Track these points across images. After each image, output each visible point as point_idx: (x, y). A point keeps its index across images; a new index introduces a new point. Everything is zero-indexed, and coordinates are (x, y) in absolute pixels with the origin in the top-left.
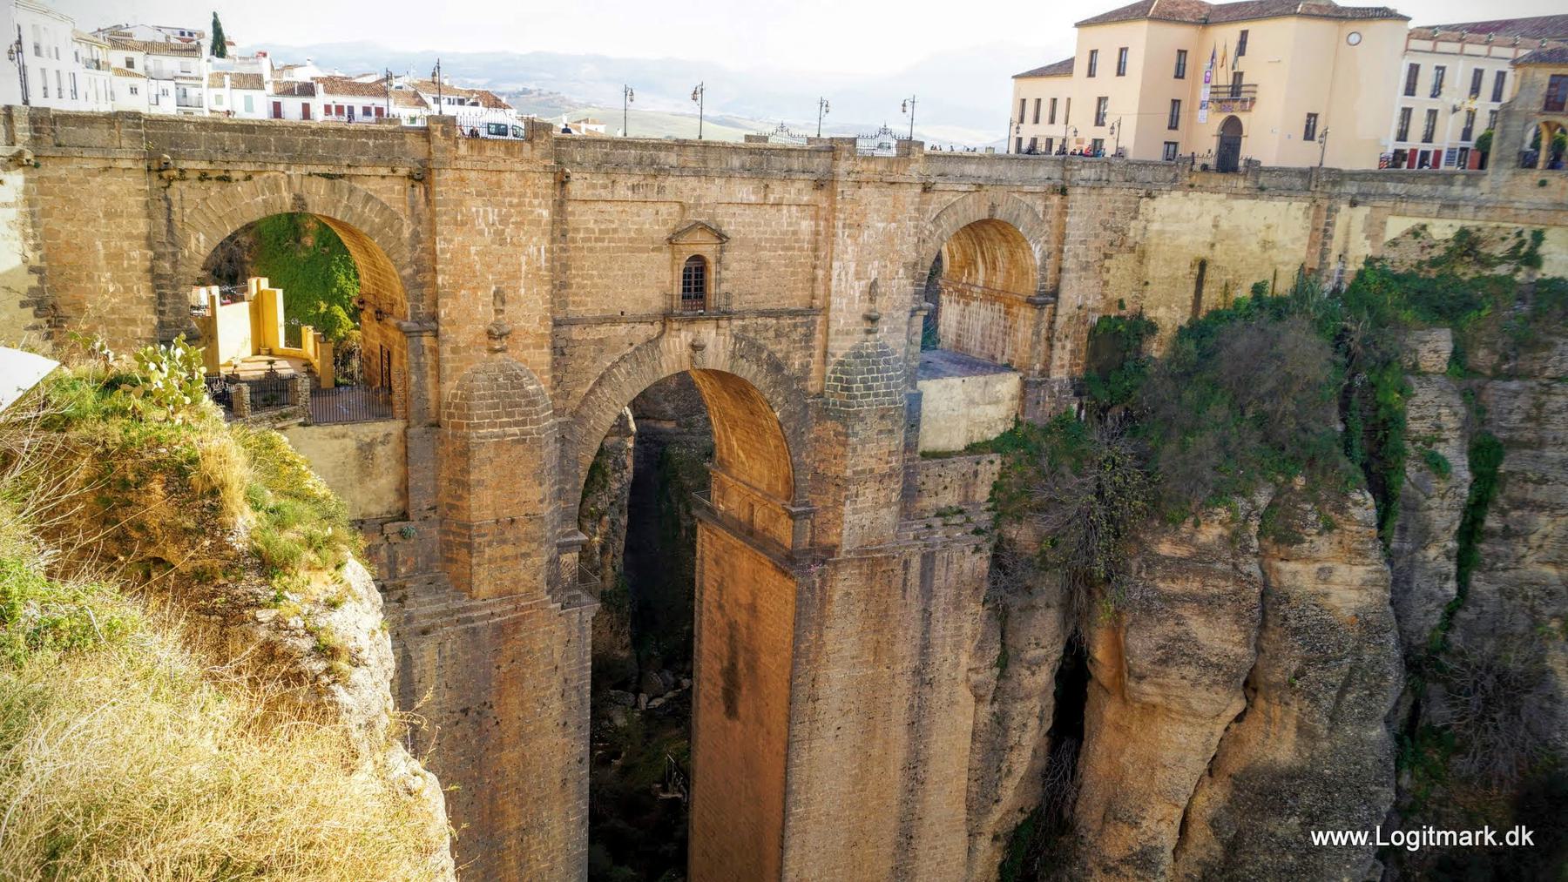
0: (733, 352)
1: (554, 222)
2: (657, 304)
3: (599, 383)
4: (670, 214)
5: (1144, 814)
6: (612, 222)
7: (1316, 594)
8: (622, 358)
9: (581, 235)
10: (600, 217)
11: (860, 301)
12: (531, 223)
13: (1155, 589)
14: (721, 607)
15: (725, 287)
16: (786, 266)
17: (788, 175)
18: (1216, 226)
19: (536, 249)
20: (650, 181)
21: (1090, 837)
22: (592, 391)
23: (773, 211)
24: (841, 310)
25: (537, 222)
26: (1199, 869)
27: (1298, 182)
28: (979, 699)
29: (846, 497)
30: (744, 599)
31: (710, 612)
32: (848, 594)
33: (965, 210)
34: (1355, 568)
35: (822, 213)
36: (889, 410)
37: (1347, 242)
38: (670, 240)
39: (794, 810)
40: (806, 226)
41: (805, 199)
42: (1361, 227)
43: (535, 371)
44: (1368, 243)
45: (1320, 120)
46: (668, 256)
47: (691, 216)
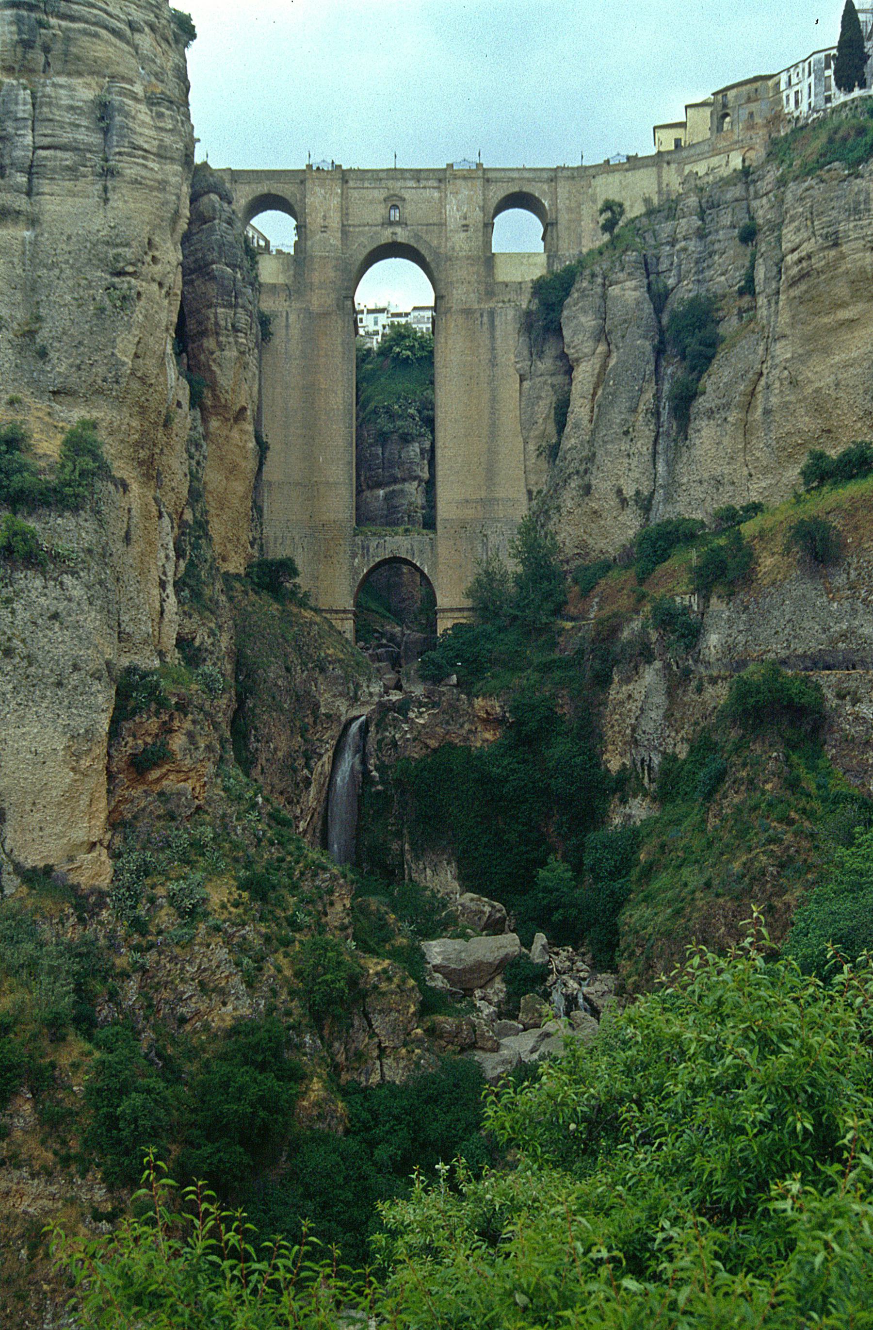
2: (380, 221)
19: (335, 202)
40: (436, 195)
41: (435, 185)
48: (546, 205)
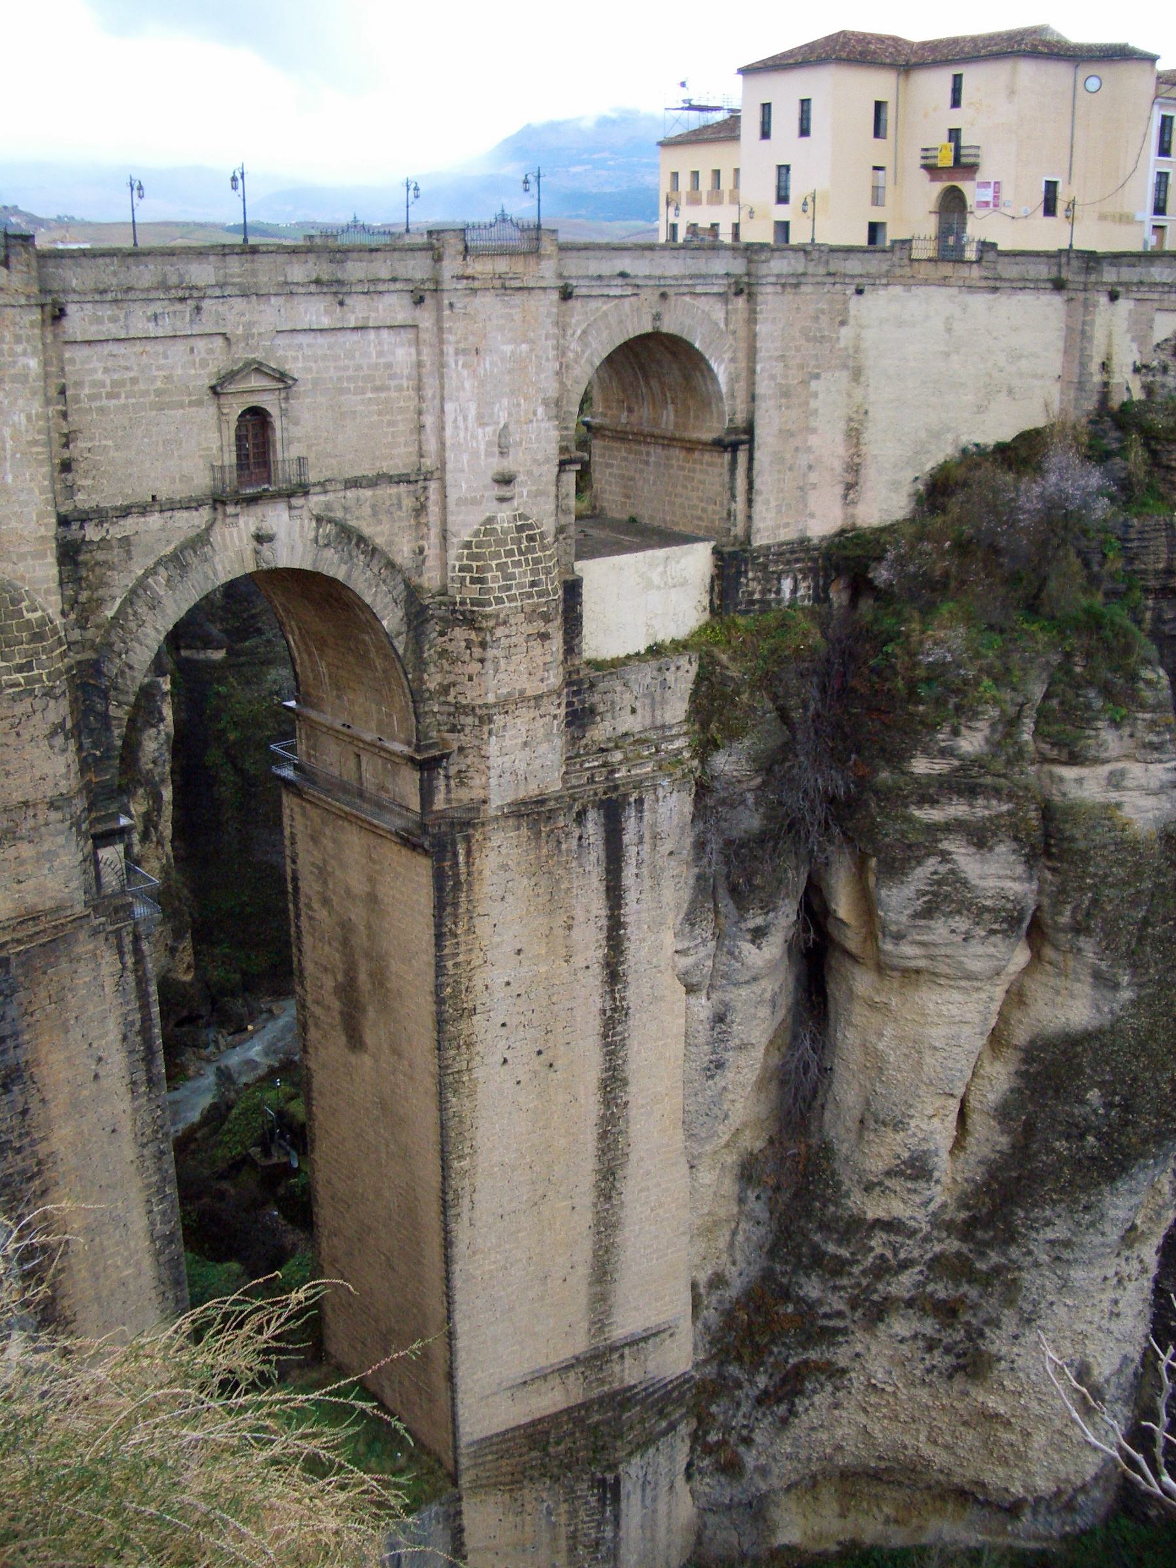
0: (316, 540)
1: (47, 376)
2: (202, 482)
3: (129, 601)
4: (210, 351)
5: (912, 1112)
6: (127, 368)
7: (1106, 807)
8: (158, 563)
9: (87, 391)
10: (109, 364)
11: (488, 454)
12: (15, 379)
13: (909, 819)
14: (326, 902)
15: (295, 451)
16: (380, 413)
17: (373, 288)
18: (949, 330)
20: (178, 307)
21: (843, 1149)
22: (121, 611)
23: (356, 336)
24: (462, 471)
25: (22, 378)
26: (983, 1168)
27: (1043, 270)
28: (691, 989)
29: (490, 733)
30: (359, 886)
31: (310, 907)
32: (505, 867)
33: (621, 322)
34: (1151, 767)
35: (424, 336)
36: (538, 605)
37: (1110, 345)
38: (213, 388)
39: (456, 1164)
40: (402, 354)
41: (401, 317)
42: (1124, 325)
43: (37, 591)
44: (1134, 346)
45: (1060, 188)
46: (213, 410)
47: (242, 354)
48: (722, 378)
